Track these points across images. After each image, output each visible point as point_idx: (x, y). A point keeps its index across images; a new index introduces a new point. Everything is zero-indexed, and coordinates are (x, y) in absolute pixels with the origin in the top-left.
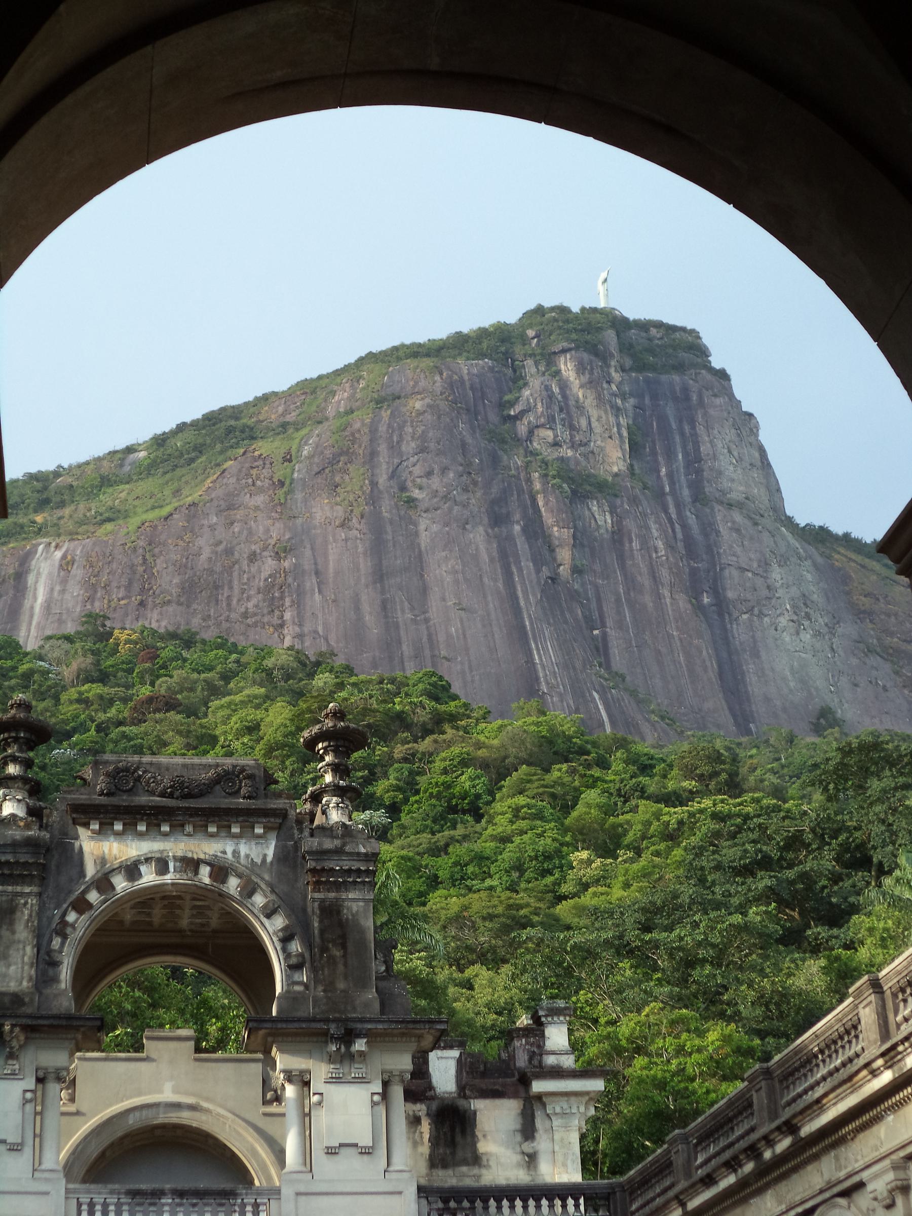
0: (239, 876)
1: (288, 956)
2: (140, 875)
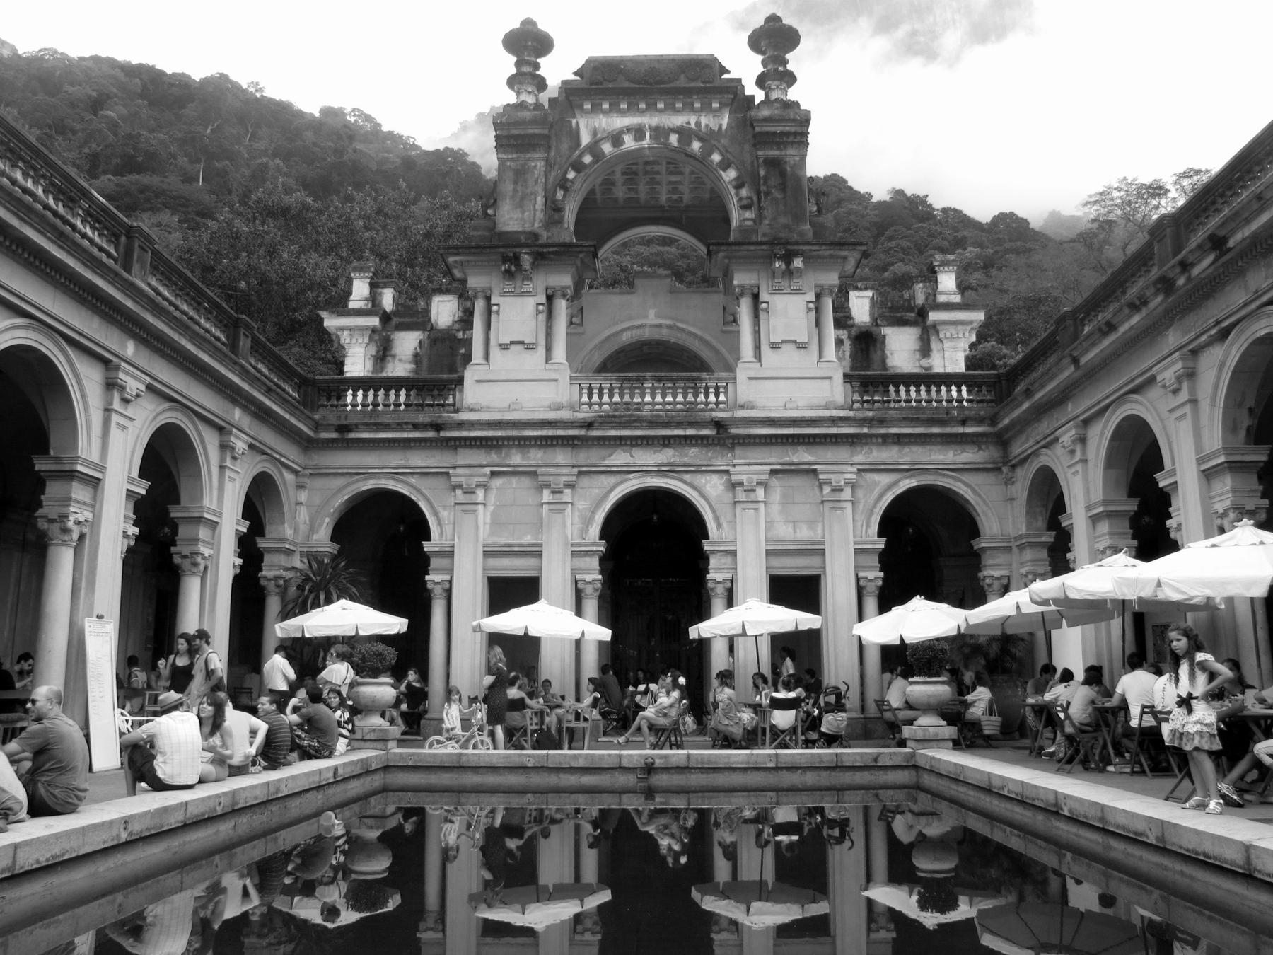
0: (701, 140)
1: (741, 199)
2: (623, 142)
